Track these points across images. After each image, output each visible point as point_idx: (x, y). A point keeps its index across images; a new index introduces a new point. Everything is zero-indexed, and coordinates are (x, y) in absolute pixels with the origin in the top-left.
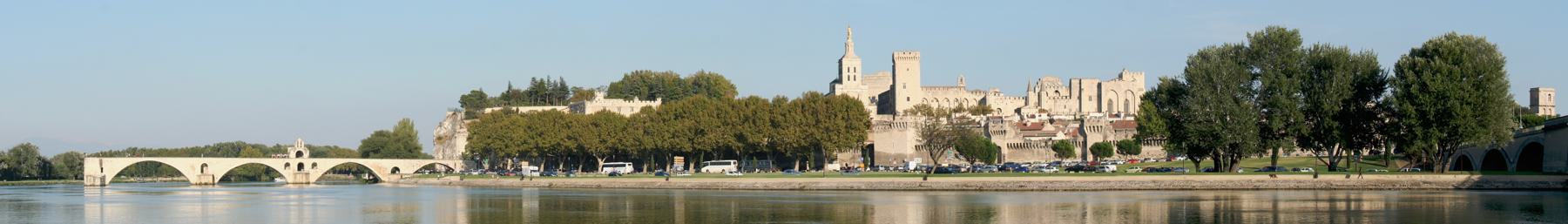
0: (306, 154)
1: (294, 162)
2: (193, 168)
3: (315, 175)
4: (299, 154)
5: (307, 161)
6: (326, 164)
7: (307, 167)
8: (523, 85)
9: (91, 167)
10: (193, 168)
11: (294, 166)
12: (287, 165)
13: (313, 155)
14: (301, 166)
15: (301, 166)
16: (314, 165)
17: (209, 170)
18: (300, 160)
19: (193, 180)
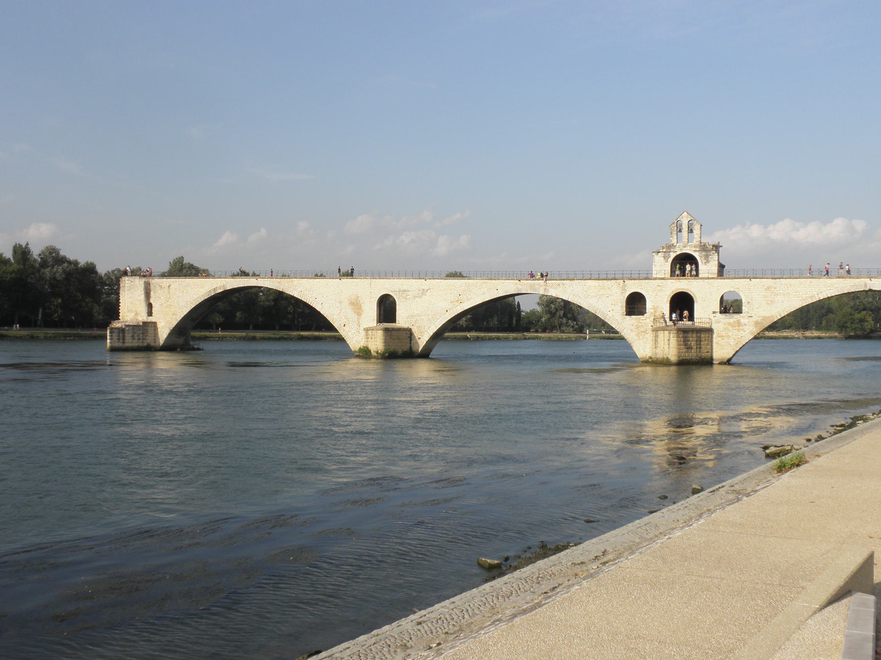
7: (705, 312)
11: (658, 301)
12: (635, 304)
14: (682, 303)
15: (682, 303)
19: (355, 340)
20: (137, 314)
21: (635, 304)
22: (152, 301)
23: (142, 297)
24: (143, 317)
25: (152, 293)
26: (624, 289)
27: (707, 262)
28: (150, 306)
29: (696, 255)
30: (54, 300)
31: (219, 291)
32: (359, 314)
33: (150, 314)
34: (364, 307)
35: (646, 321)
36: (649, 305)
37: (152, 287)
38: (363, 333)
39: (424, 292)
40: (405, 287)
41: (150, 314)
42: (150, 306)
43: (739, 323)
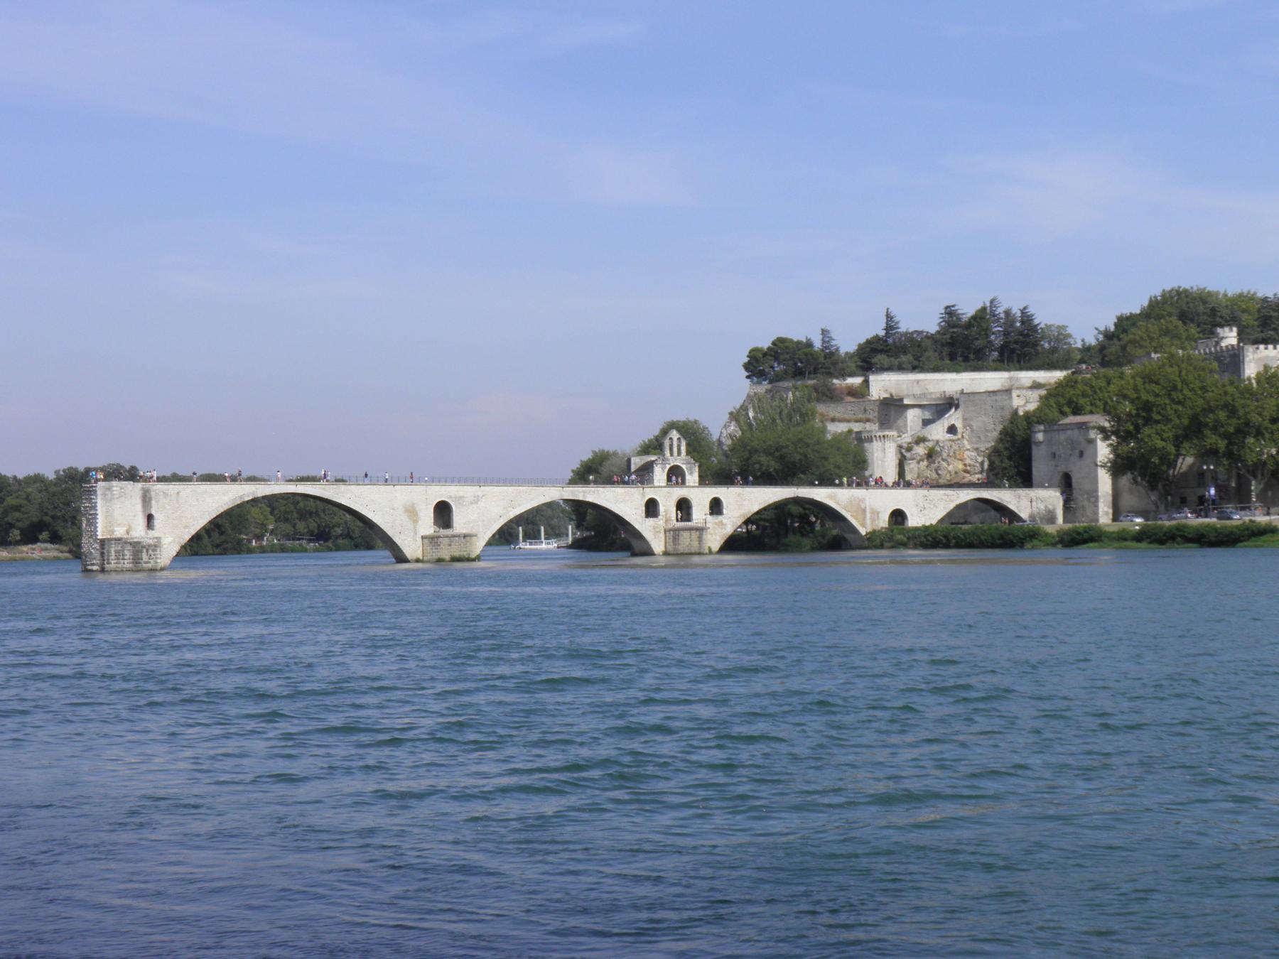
0: (692, 477)
1: (667, 499)
2: (412, 512)
3: (718, 532)
4: (675, 475)
6: (746, 501)
7: (700, 513)
8: (922, 319)
9: (115, 514)
10: (412, 512)
11: (667, 506)
12: (651, 508)
13: (704, 481)
16: (716, 507)
17: (461, 522)
18: (679, 493)
19: (411, 546)
21: (651, 508)
23: (139, 507)
24: (139, 531)
26: (643, 495)
27: (691, 474)
28: (150, 518)
29: (684, 467)
30: (41, 515)
32: (416, 522)
34: (421, 514)
35: (659, 522)
36: (661, 509)
38: (419, 540)
39: (477, 500)
40: (461, 494)
42: (150, 518)
43: (721, 523)
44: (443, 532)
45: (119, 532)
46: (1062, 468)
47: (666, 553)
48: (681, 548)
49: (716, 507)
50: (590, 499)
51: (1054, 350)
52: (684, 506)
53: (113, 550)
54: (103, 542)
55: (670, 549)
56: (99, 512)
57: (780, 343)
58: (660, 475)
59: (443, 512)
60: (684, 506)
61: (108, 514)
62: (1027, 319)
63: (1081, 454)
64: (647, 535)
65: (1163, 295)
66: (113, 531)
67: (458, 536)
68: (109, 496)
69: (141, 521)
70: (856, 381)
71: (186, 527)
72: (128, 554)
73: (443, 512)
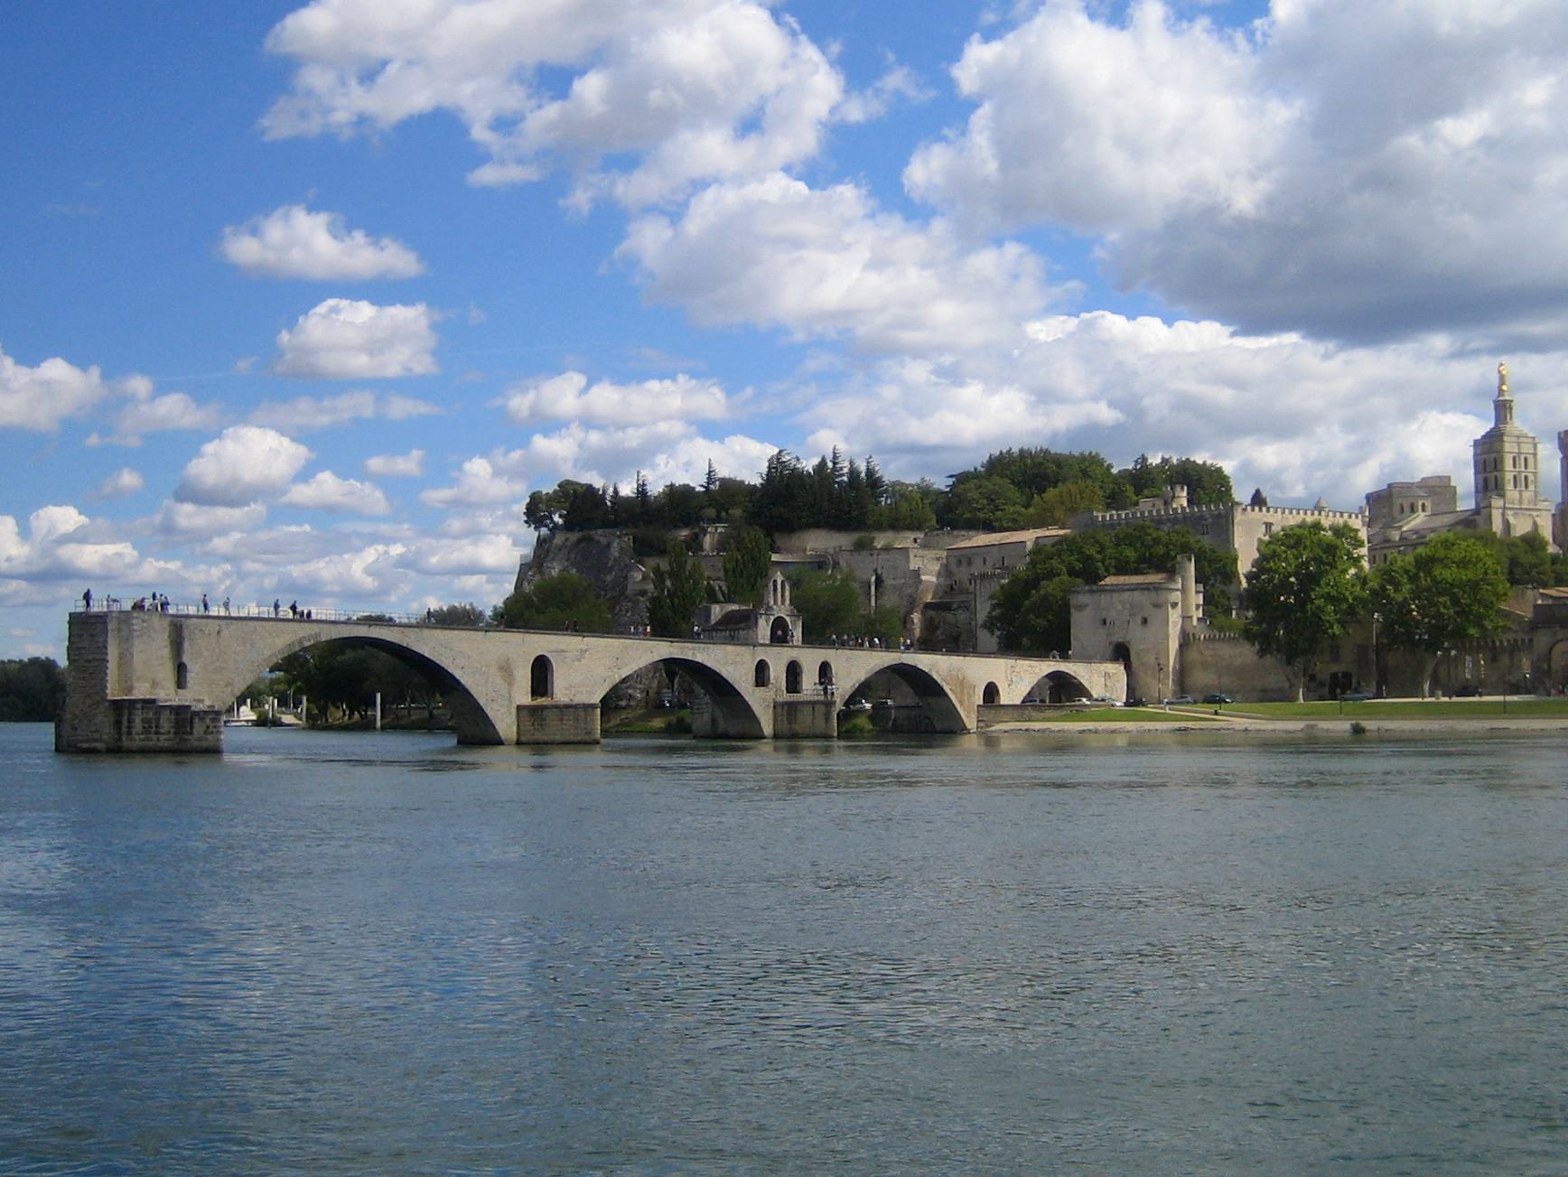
1: (777, 661)
2: (506, 670)
5: (810, 659)
6: (855, 666)
7: (809, 681)
11: (777, 673)
12: (761, 671)
16: (825, 670)
19: (506, 725)
20: (155, 684)
21: (761, 671)
22: (185, 659)
23: (166, 652)
24: (167, 694)
25: (186, 645)
26: (754, 655)
28: (181, 669)
31: (307, 644)
32: (510, 684)
33: (181, 683)
37: (186, 632)
38: (514, 711)
40: (563, 647)
41: (181, 683)
42: (181, 669)
44: (541, 701)
45: (138, 694)
46: (1118, 638)
47: (776, 736)
48: (797, 728)
49: (825, 670)
50: (699, 658)
51: (894, 508)
52: (794, 671)
53: (138, 720)
54: (118, 705)
55: (784, 728)
56: (110, 657)
57: (565, 485)
58: (764, 629)
59: (541, 671)
60: (794, 671)
61: (125, 660)
62: (870, 472)
63: (1145, 621)
64: (758, 709)
65: (1021, 451)
66: (130, 690)
67: (556, 707)
68: (124, 633)
69: (167, 674)
70: (684, 533)
71: (228, 684)
72: (166, 723)
73: (541, 671)
